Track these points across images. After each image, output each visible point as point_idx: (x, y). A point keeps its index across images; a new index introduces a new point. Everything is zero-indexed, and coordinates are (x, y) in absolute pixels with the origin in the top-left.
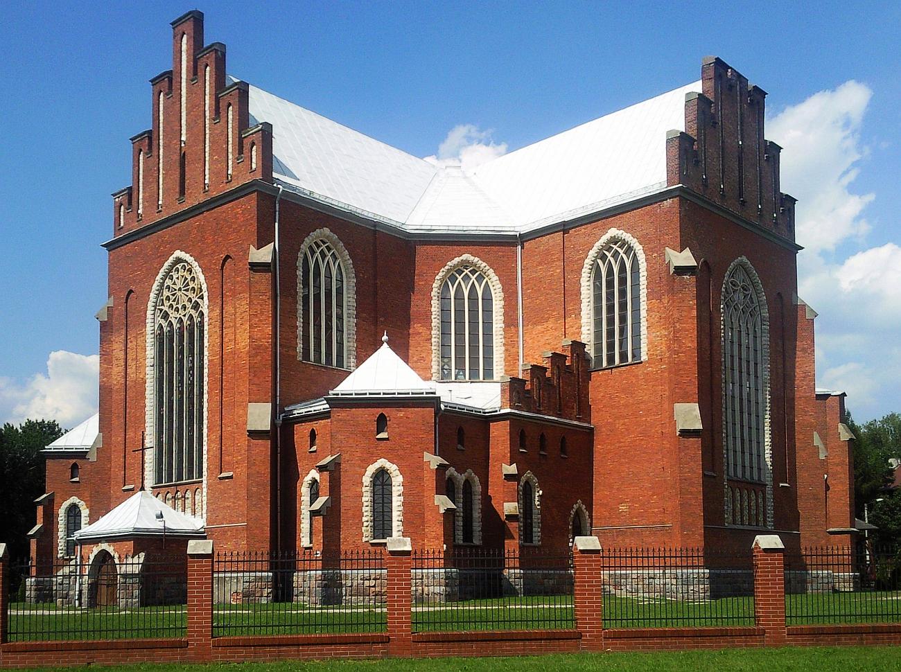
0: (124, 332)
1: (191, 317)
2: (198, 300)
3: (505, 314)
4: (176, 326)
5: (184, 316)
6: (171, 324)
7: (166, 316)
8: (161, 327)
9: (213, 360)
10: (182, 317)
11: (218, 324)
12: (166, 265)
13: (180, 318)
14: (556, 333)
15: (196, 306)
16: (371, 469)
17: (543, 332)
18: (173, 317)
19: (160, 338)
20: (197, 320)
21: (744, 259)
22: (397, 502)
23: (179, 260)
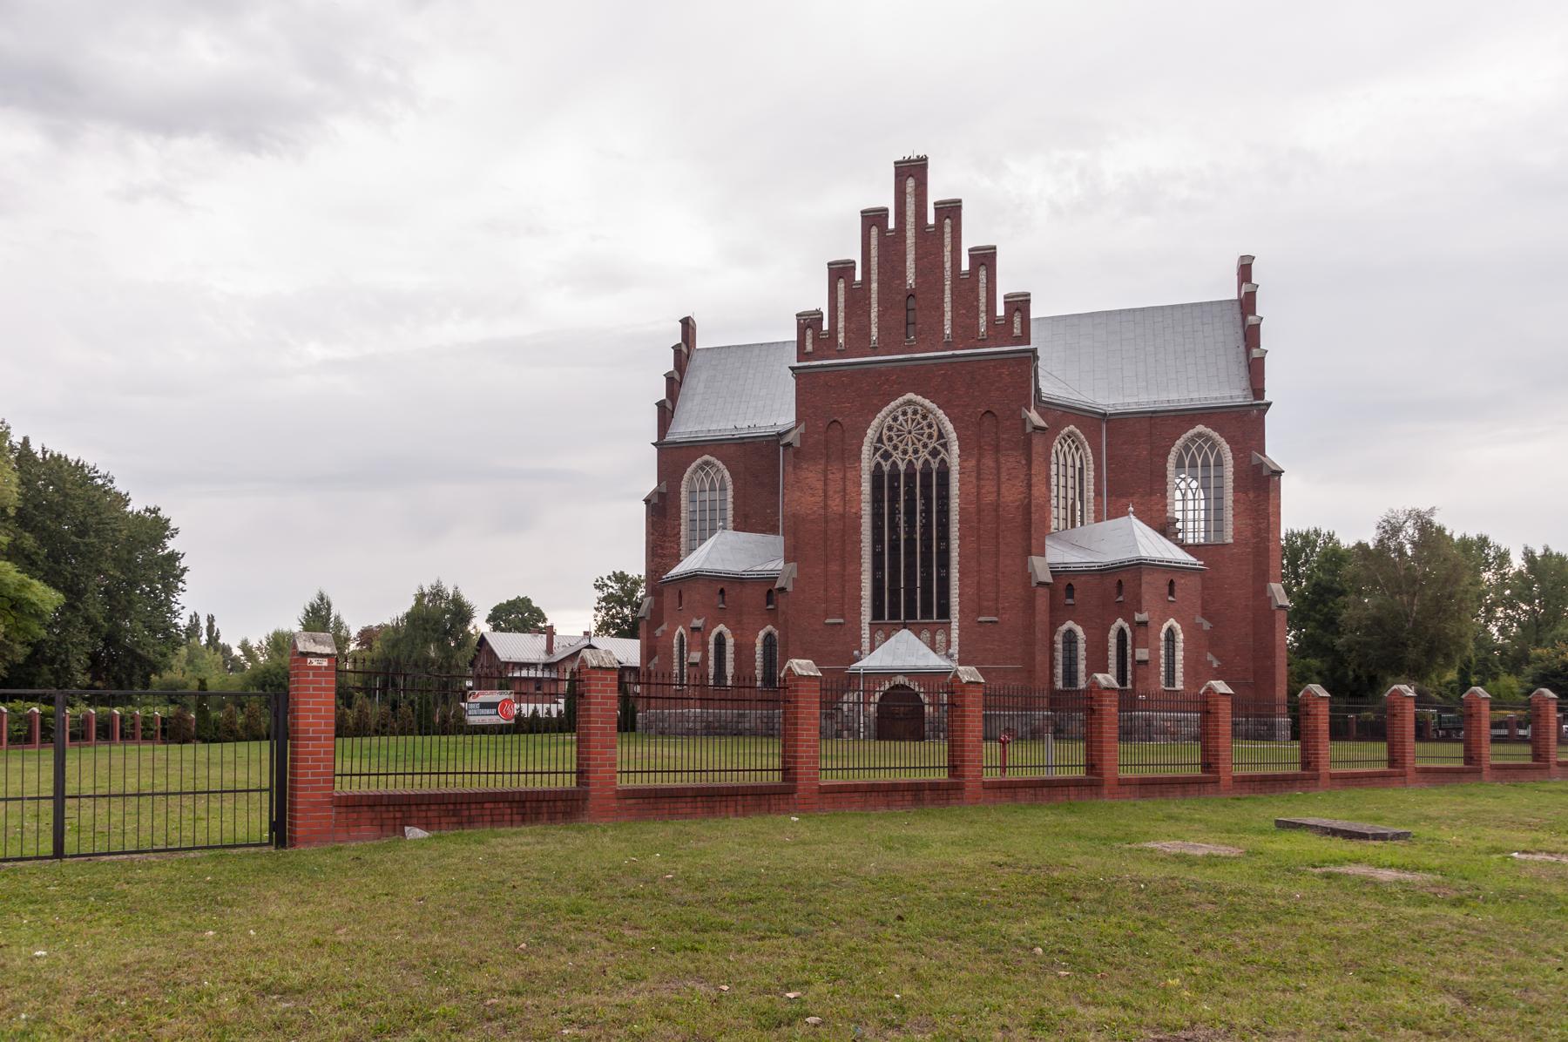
0: (823, 462)
1: (926, 461)
2: (939, 448)
4: (902, 467)
5: (917, 459)
6: (894, 463)
7: (886, 455)
8: (878, 464)
9: (965, 509)
10: (914, 461)
11: (974, 474)
12: (893, 404)
13: (910, 461)
14: (1142, 508)
15: (935, 453)
16: (1165, 627)
18: (897, 456)
20: (935, 465)
21: (1072, 427)
22: (1179, 655)
23: (910, 403)
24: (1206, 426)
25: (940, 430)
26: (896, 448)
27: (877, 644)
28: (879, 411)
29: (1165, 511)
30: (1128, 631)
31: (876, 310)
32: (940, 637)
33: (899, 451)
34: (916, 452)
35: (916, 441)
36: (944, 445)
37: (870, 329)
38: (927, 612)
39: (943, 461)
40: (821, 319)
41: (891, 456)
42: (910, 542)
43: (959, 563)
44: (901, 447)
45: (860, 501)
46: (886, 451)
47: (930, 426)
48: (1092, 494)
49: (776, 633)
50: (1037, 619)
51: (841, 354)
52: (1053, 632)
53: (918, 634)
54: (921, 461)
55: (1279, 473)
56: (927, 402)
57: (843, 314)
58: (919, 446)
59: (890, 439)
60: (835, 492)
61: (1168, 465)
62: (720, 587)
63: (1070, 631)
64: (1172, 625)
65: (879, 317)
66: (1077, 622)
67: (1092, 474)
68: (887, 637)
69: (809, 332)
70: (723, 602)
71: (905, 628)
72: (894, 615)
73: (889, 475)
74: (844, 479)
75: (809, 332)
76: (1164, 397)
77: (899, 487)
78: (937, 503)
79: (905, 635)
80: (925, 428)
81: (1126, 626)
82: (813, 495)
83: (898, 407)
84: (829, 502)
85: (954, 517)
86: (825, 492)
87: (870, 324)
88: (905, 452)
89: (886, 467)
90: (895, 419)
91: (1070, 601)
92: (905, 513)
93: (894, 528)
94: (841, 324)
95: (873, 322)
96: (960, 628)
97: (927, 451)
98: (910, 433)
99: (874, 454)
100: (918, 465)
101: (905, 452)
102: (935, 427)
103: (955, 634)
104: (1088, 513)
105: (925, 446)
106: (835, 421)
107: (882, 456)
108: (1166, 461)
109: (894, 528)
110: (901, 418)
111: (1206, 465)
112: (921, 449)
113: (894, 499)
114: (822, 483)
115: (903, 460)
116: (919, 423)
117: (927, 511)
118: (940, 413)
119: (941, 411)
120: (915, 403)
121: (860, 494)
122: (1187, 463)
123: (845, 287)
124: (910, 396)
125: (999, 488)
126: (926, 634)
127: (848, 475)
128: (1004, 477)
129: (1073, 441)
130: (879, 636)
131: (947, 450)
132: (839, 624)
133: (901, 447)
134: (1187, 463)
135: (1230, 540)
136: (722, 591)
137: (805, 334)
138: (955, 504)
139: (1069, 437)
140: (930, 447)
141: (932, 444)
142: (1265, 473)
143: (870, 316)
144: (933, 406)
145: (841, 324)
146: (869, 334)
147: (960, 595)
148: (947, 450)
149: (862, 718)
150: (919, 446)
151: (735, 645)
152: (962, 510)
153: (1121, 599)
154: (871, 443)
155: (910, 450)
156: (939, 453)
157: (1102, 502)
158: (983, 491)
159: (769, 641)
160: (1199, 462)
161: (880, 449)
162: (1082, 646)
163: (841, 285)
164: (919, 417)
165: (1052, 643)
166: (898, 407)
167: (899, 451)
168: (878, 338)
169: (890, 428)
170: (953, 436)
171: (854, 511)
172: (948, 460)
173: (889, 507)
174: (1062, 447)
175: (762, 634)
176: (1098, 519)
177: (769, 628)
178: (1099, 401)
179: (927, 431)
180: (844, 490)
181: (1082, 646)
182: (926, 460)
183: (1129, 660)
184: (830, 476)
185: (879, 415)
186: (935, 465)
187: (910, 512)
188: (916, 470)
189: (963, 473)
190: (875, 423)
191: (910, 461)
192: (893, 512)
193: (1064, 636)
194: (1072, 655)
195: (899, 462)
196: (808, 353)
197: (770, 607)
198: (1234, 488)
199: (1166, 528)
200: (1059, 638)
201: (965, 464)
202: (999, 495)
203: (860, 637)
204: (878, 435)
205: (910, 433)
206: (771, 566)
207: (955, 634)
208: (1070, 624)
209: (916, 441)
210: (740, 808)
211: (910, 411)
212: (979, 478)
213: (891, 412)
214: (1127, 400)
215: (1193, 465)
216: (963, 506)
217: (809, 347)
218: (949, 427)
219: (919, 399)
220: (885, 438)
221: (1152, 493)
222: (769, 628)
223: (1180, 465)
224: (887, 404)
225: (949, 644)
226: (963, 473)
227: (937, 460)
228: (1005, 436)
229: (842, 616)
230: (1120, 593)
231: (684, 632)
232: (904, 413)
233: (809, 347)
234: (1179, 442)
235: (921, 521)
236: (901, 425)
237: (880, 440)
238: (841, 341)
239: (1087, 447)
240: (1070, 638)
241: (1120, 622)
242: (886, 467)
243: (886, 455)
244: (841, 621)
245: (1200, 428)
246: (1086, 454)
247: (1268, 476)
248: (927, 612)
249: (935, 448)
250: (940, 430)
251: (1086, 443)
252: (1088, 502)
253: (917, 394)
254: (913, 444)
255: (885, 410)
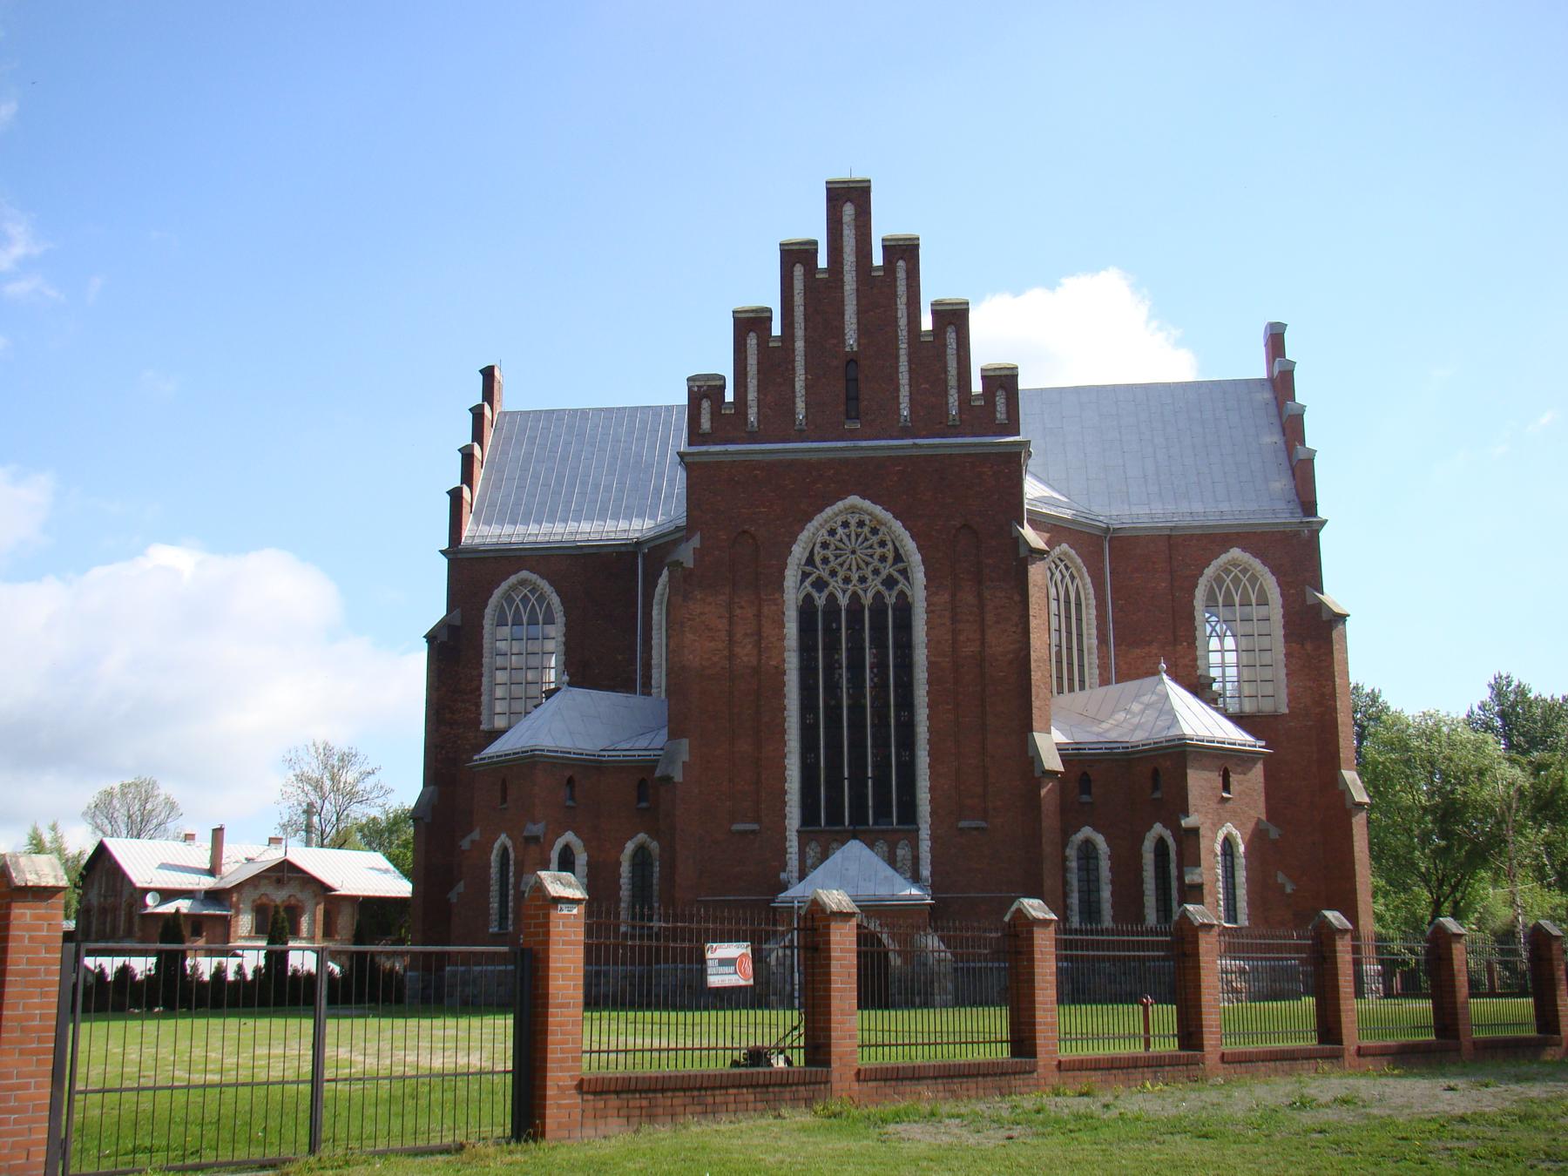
1: (878, 596)
2: (896, 575)
3: (1098, 628)
4: (843, 601)
6: (832, 598)
7: (820, 585)
8: (808, 599)
12: (829, 511)
13: (855, 593)
16: (1220, 838)
17: (1144, 657)
18: (835, 585)
19: (807, 611)
20: (890, 599)
23: (853, 510)
24: (1244, 549)
25: (896, 549)
26: (833, 573)
27: (809, 862)
28: (810, 519)
29: (1195, 667)
30: (1171, 841)
31: (803, 377)
32: (903, 852)
33: (839, 579)
34: (863, 580)
35: (863, 565)
36: (904, 572)
37: (794, 403)
38: (883, 811)
39: (902, 595)
40: (723, 387)
41: (826, 584)
42: (857, 709)
43: (930, 742)
44: (841, 573)
45: (783, 649)
46: (819, 578)
47: (883, 544)
48: (1095, 642)
49: (654, 846)
50: (1044, 824)
51: (753, 438)
52: (1065, 844)
53: (871, 845)
54: (870, 594)
55: (1342, 618)
56: (878, 510)
57: (755, 382)
58: (868, 572)
59: (825, 561)
60: (746, 635)
61: (1196, 603)
62: (568, 773)
63: (1088, 842)
64: (1229, 834)
65: (807, 387)
66: (1097, 829)
67: (1093, 612)
68: (824, 856)
69: (706, 404)
70: (572, 798)
71: (855, 837)
72: (835, 817)
73: (824, 613)
74: (758, 616)
75: (706, 404)
76: (1184, 507)
77: (839, 629)
78: (895, 653)
79: (855, 848)
80: (876, 546)
81: (1168, 835)
82: (713, 639)
83: (837, 515)
84: (737, 650)
85: (921, 675)
86: (731, 634)
87: (794, 397)
88: (847, 580)
89: (820, 600)
90: (832, 532)
91: (1085, 798)
92: (848, 668)
93: (832, 688)
94: (752, 395)
95: (798, 394)
96: (934, 838)
97: (878, 580)
98: (853, 552)
99: (802, 582)
100: (867, 600)
101: (847, 580)
102: (890, 546)
103: (925, 846)
104: (1090, 668)
105: (876, 572)
106: (745, 532)
107: (813, 585)
108: (1192, 596)
109: (832, 688)
110: (840, 531)
111: (1245, 603)
112: (870, 577)
113: (832, 646)
114: (725, 621)
115: (844, 592)
116: (866, 539)
117: (881, 666)
118: (897, 526)
119: (899, 524)
120: (861, 511)
121: (782, 638)
122: (1220, 600)
123: (758, 345)
124: (854, 500)
125: (983, 632)
126: (882, 846)
127: (765, 610)
128: (990, 618)
129: (1067, 568)
130: (813, 851)
131: (907, 578)
132: (753, 832)
133: (841, 573)
134: (1220, 600)
135: (1285, 710)
136: (570, 781)
137: (699, 407)
138: (921, 656)
139: (1062, 561)
140: (884, 574)
141: (887, 569)
142: (1325, 617)
143: (794, 387)
144: (887, 516)
145: (752, 395)
146: (793, 413)
147: (932, 789)
148: (907, 578)
149: (796, 975)
150: (868, 572)
151: (589, 864)
152: (931, 666)
153: (1157, 795)
154: (799, 565)
155: (855, 577)
156: (896, 582)
157: (1108, 652)
158: (962, 638)
159: (641, 859)
160: (1237, 600)
161: (810, 574)
162: (1105, 865)
163: (752, 341)
164: (866, 530)
165: (1065, 859)
166: (837, 515)
167: (839, 579)
168: (806, 417)
169: (825, 545)
170: (916, 558)
171: (773, 663)
172: (909, 593)
173: (824, 657)
174: (1052, 574)
175: (630, 847)
176: (1104, 681)
177: (642, 837)
178: (1096, 509)
179: (879, 551)
180: (759, 633)
181: (1105, 865)
182: (878, 593)
183: (1174, 884)
184: (738, 611)
185: (809, 526)
186: (890, 599)
187: (856, 666)
188: (863, 607)
189: (933, 612)
190: (804, 536)
191: (855, 593)
192: (831, 667)
193: (1079, 849)
194: (1092, 877)
195: (839, 595)
196: (704, 435)
197: (644, 805)
198: (1285, 636)
199: (1200, 688)
200: (1071, 852)
201: (935, 599)
202: (983, 643)
203: (784, 851)
204: (806, 554)
205: (853, 552)
206: (643, 743)
207: (925, 846)
208: (1087, 832)
209: (863, 565)
210: (981, 1092)
211: (853, 521)
212: (954, 620)
213: (826, 522)
214: (1136, 510)
215: (1229, 604)
216: (933, 659)
217: (706, 424)
218: (910, 546)
219: (867, 504)
220: (817, 559)
221: (1176, 641)
222: (642, 837)
223: (1211, 602)
224: (821, 510)
225: (916, 860)
226: (933, 612)
227: (894, 593)
228: (990, 561)
229: (757, 820)
230: (1156, 787)
231: (509, 844)
232: (845, 525)
233: (706, 424)
234: (1209, 572)
235: (871, 680)
236: (841, 540)
237: (810, 561)
238: (752, 418)
239: (1086, 575)
240: (1088, 850)
241: (1158, 829)
242: (820, 600)
243: (820, 585)
244: (755, 827)
245: (1235, 553)
246: (1084, 585)
247: (1330, 621)
248: (883, 811)
249: (890, 576)
250: (896, 549)
251: (1084, 569)
252: (1089, 654)
253: (864, 497)
254: (859, 568)
255: (818, 519)
